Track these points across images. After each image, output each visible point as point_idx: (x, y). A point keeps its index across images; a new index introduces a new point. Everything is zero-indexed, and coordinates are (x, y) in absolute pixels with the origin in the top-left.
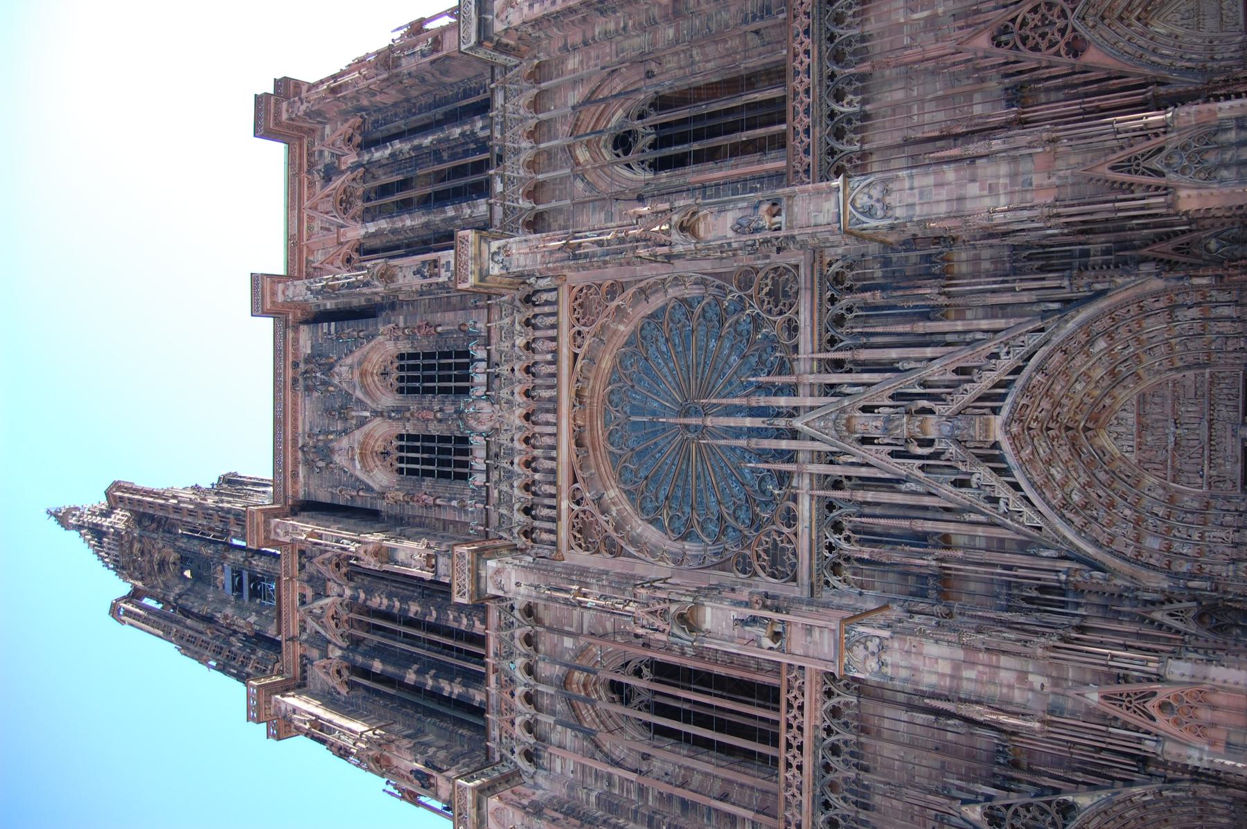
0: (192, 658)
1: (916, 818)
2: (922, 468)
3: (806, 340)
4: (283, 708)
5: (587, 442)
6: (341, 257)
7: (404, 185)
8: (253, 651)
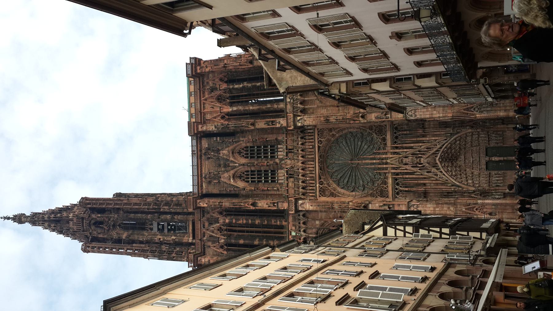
0: (139, 257)
2: (419, 169)
4: (203, 260)
5: (323, 170)
6: (220, 116)
7: (245, 96)
8: (175, 249)
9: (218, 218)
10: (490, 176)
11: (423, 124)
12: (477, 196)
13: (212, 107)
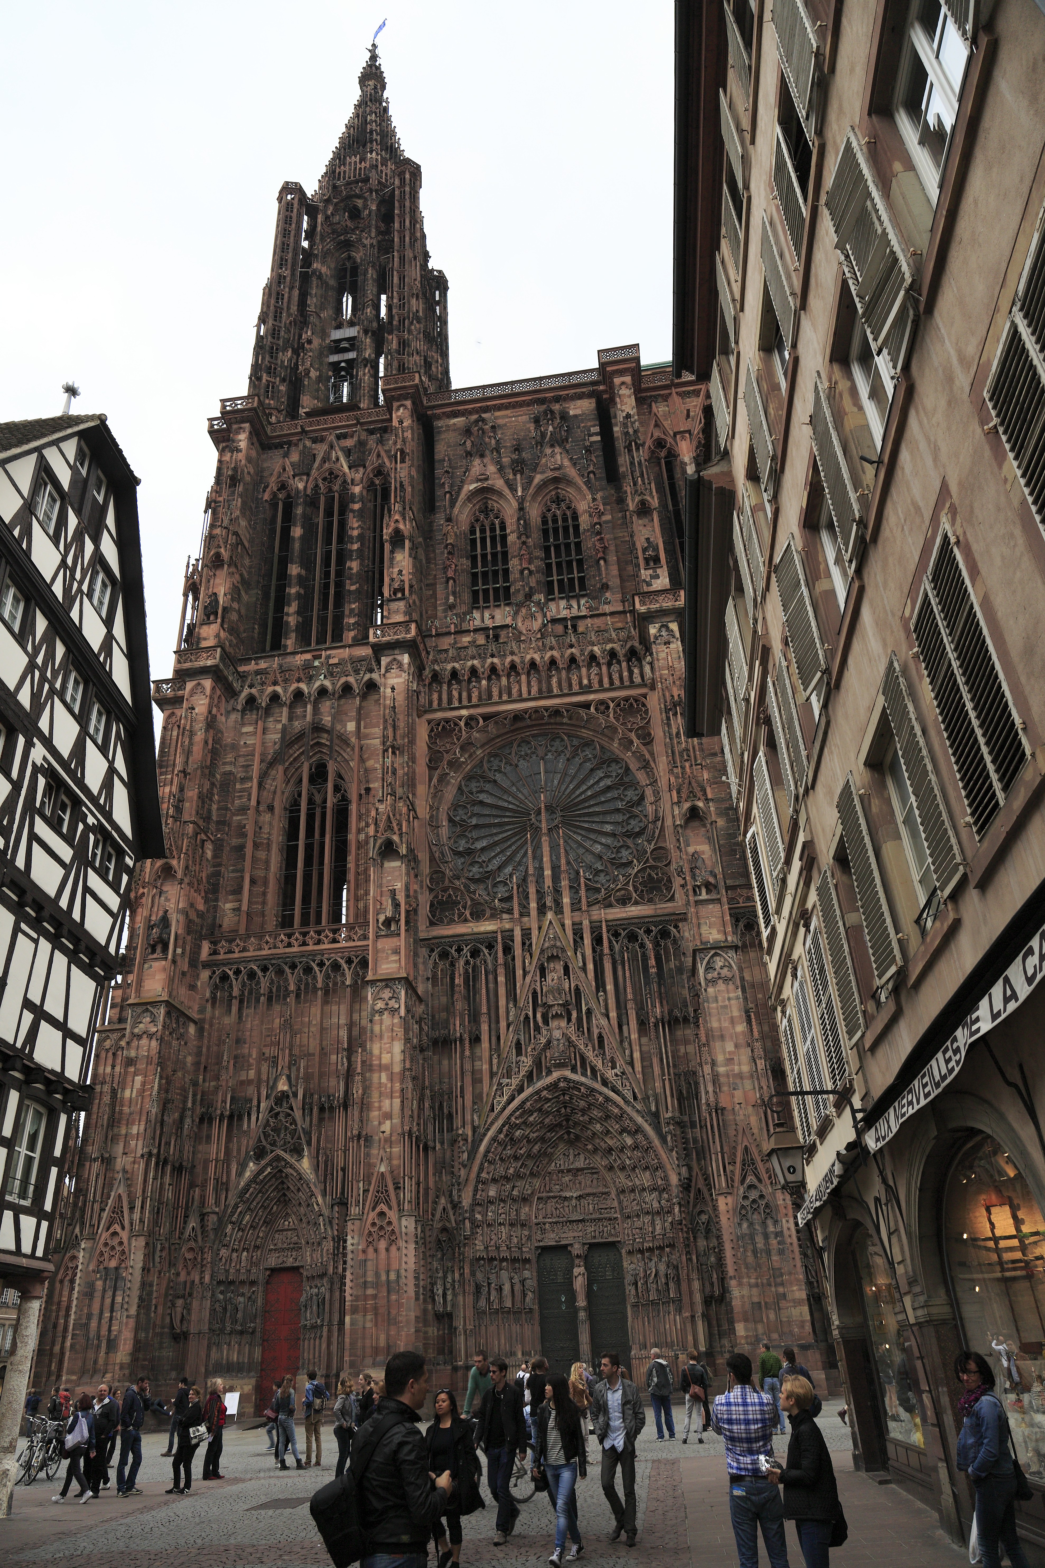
1: (269, 1039)
2: (527, 1017)
3: (617, 913)
6: (663, 436)
8: (283, 380)
9: (364, 467)
10: (515, 1260)
11: (686, 1020)
12: (441, 1220)
13: (688, 411)
